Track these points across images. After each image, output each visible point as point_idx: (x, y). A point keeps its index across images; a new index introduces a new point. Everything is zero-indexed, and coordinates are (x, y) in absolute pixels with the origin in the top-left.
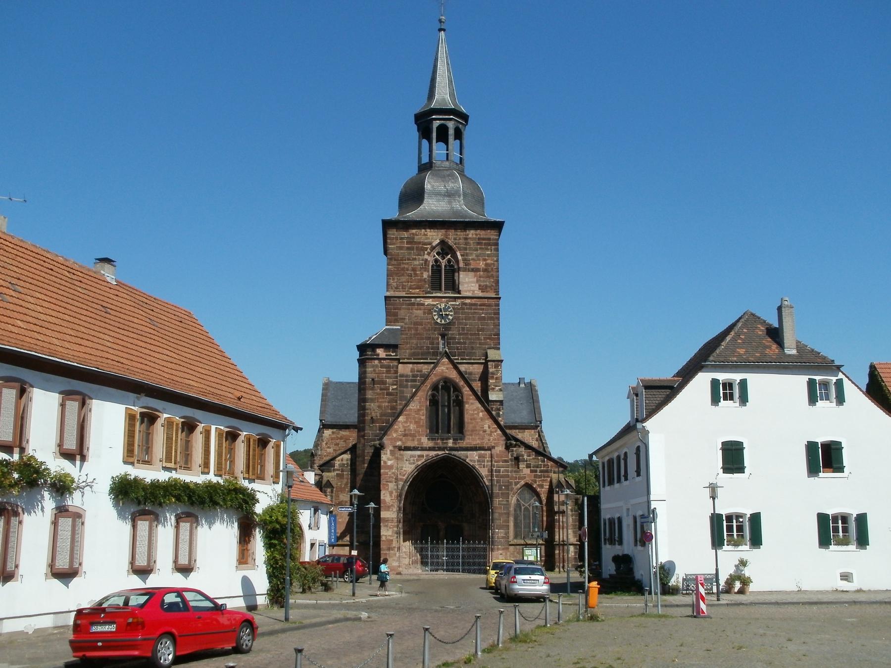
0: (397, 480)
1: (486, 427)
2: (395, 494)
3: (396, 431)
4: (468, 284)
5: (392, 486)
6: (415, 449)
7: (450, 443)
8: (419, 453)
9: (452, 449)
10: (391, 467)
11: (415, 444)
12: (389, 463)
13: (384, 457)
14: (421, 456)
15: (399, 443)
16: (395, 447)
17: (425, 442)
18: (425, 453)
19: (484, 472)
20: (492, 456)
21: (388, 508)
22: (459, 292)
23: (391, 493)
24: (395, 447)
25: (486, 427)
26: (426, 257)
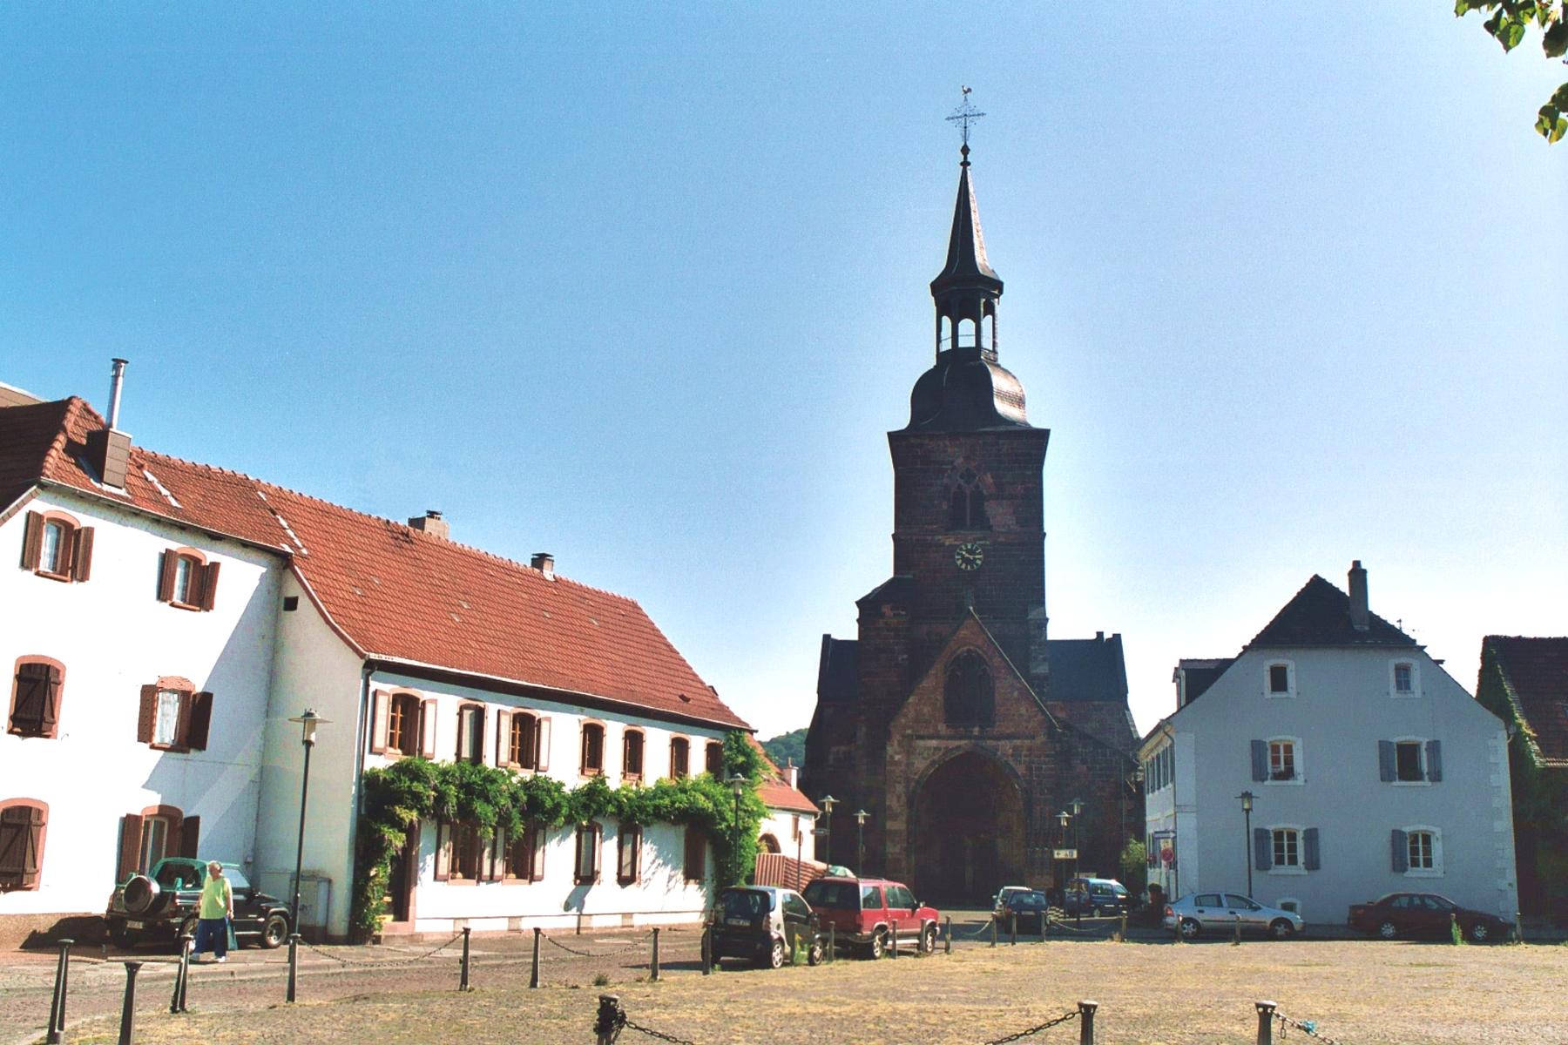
0: (908, 780)
1: (1023, 711)
2: (903, 798)
3: (905, 716)
4: (1000, 515)
5: (900, 788)
6: (931, 737)
7: (976, 730)
8: (934, 743)
9: (977, 738)
10: (897, 763)
11: (931, 731)
12: (897, 757)
13: (890, 750)
14: (937, 749)
15: (909, 731)
16: (904, 736)
17: (942, 728)
18: (943, 744)
19: (1021, 770)
20: (1030, 749)
21: (895, 817)
22: (990, 528)
23: (899, 797)
24: (904, 736)
25: (1023, 711)
26: (946, 481)
